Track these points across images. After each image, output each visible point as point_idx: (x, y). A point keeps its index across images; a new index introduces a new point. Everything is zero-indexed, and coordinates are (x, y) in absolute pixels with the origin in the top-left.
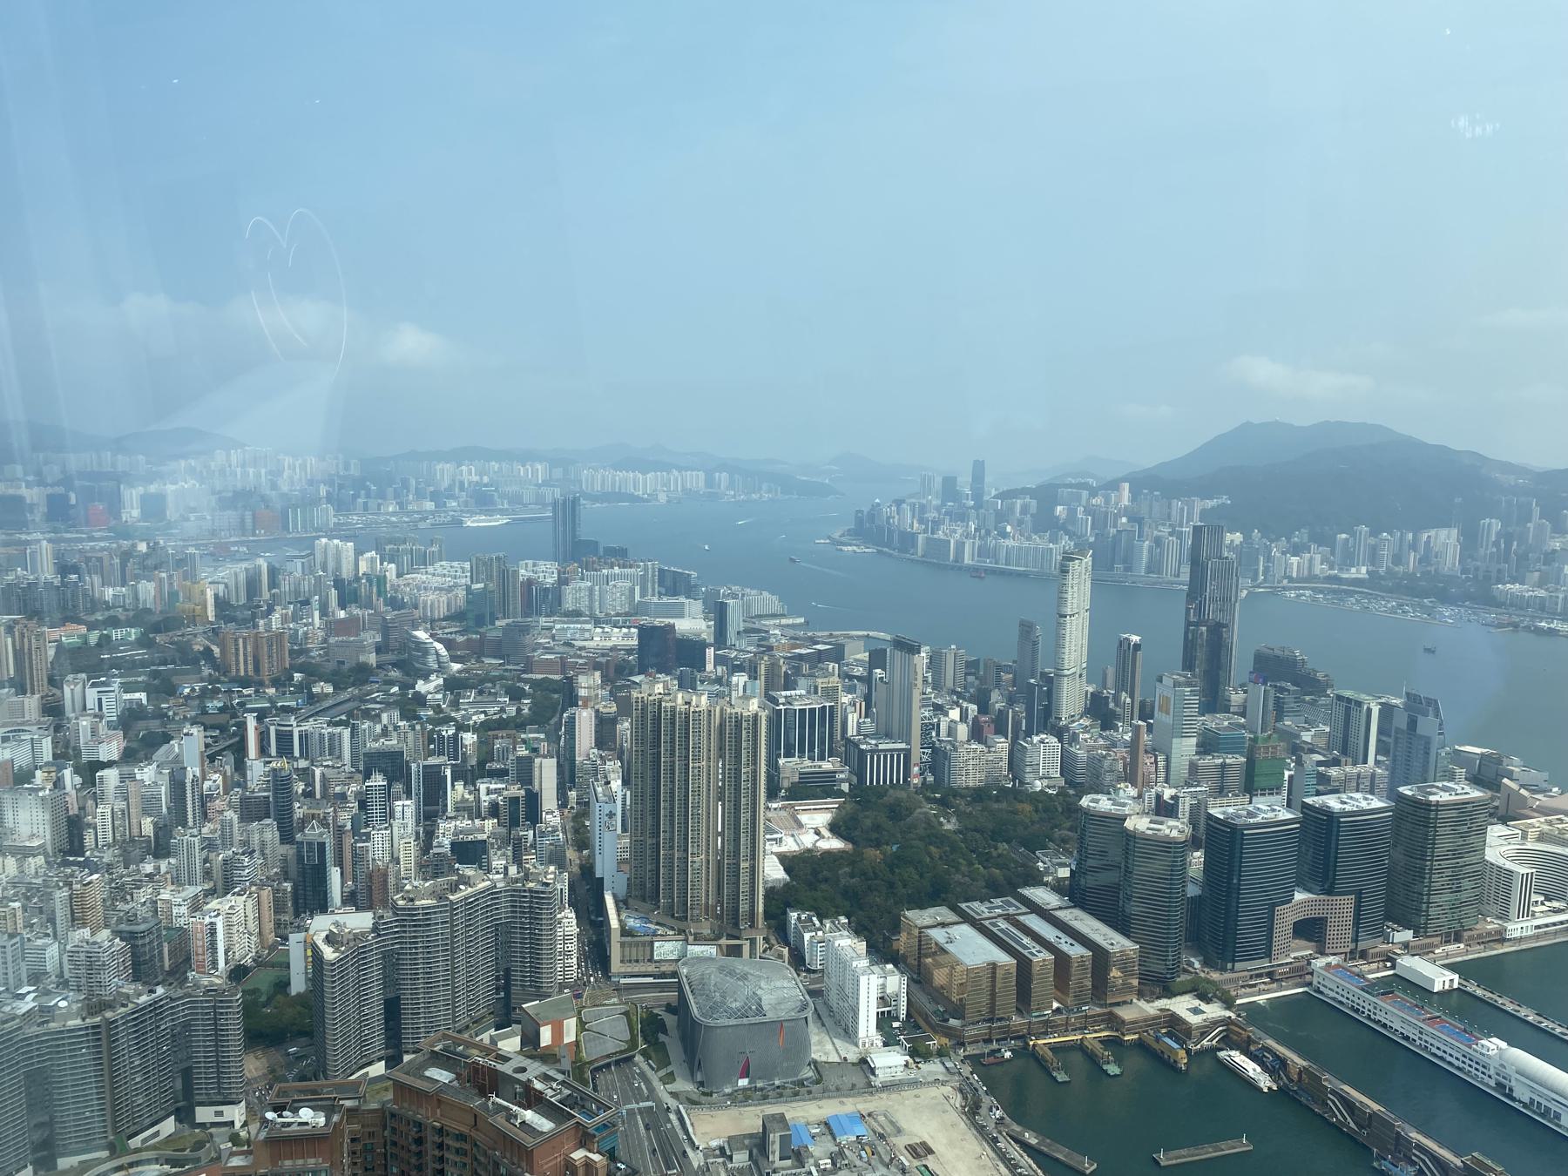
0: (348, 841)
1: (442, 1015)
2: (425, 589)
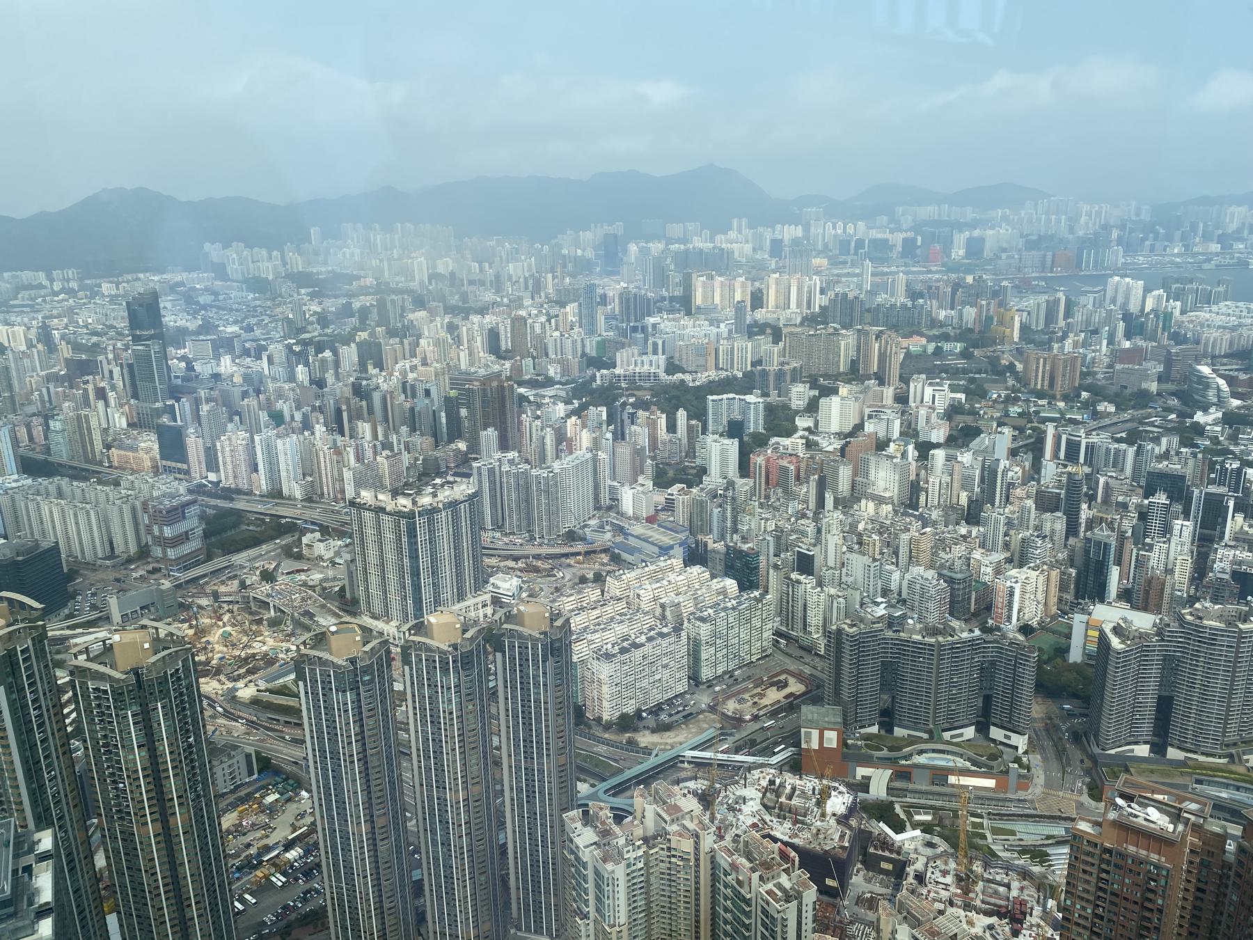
0: (1129, 545)
1: (1214, 727)
2: (1208, 326)
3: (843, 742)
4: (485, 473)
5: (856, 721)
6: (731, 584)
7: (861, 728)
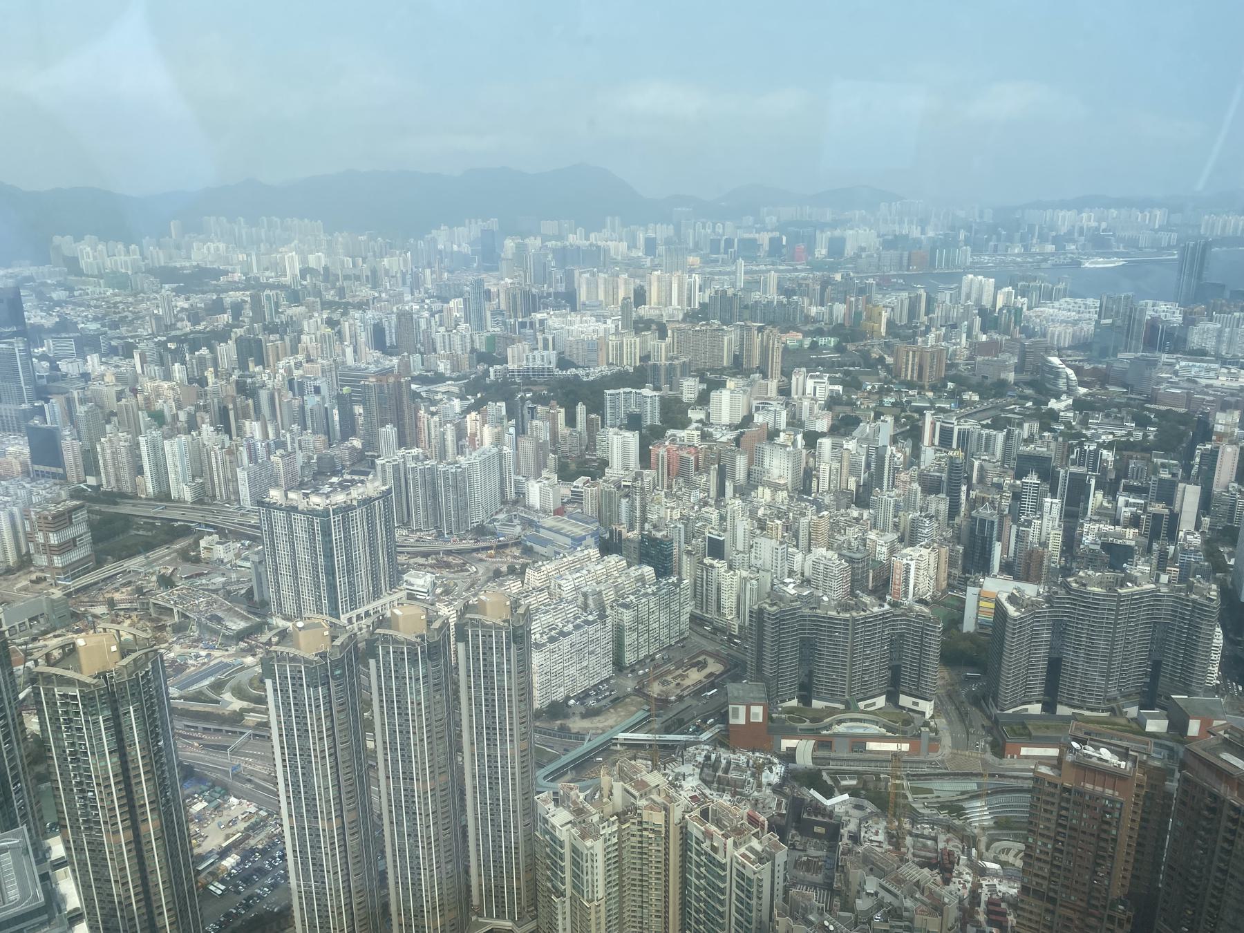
2: (1053, 320)
3: (768, 716)
4: (389, 470)
5: (778, 696)
6: (648, 571)
7: (782, 702)
